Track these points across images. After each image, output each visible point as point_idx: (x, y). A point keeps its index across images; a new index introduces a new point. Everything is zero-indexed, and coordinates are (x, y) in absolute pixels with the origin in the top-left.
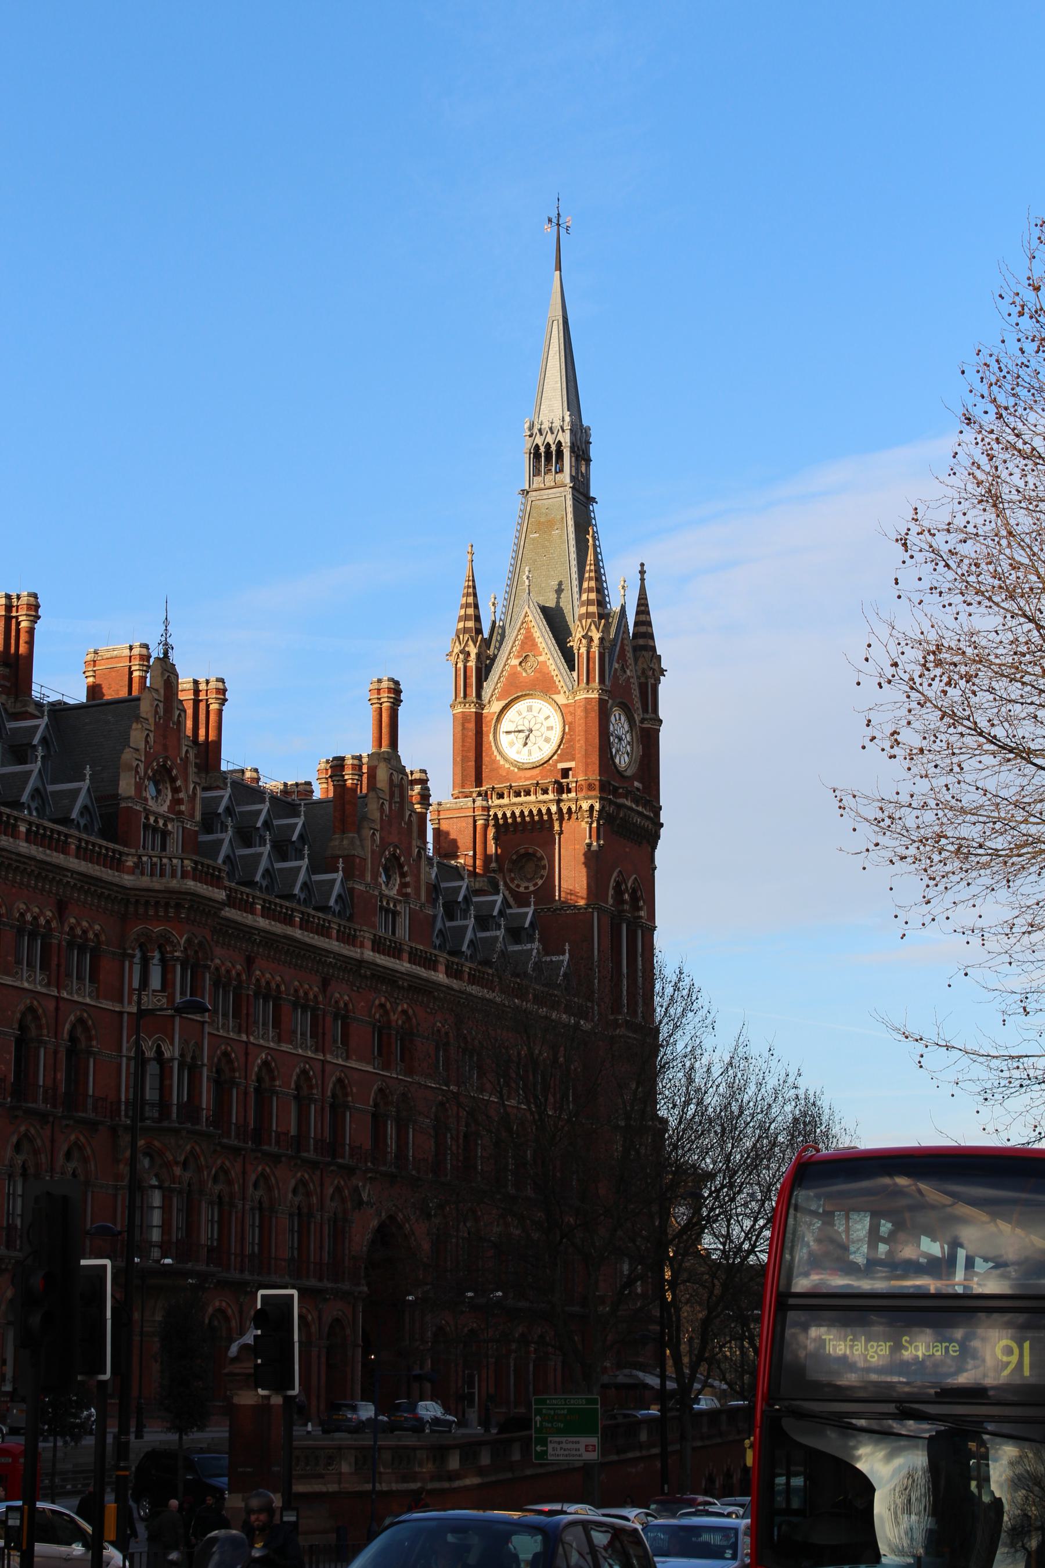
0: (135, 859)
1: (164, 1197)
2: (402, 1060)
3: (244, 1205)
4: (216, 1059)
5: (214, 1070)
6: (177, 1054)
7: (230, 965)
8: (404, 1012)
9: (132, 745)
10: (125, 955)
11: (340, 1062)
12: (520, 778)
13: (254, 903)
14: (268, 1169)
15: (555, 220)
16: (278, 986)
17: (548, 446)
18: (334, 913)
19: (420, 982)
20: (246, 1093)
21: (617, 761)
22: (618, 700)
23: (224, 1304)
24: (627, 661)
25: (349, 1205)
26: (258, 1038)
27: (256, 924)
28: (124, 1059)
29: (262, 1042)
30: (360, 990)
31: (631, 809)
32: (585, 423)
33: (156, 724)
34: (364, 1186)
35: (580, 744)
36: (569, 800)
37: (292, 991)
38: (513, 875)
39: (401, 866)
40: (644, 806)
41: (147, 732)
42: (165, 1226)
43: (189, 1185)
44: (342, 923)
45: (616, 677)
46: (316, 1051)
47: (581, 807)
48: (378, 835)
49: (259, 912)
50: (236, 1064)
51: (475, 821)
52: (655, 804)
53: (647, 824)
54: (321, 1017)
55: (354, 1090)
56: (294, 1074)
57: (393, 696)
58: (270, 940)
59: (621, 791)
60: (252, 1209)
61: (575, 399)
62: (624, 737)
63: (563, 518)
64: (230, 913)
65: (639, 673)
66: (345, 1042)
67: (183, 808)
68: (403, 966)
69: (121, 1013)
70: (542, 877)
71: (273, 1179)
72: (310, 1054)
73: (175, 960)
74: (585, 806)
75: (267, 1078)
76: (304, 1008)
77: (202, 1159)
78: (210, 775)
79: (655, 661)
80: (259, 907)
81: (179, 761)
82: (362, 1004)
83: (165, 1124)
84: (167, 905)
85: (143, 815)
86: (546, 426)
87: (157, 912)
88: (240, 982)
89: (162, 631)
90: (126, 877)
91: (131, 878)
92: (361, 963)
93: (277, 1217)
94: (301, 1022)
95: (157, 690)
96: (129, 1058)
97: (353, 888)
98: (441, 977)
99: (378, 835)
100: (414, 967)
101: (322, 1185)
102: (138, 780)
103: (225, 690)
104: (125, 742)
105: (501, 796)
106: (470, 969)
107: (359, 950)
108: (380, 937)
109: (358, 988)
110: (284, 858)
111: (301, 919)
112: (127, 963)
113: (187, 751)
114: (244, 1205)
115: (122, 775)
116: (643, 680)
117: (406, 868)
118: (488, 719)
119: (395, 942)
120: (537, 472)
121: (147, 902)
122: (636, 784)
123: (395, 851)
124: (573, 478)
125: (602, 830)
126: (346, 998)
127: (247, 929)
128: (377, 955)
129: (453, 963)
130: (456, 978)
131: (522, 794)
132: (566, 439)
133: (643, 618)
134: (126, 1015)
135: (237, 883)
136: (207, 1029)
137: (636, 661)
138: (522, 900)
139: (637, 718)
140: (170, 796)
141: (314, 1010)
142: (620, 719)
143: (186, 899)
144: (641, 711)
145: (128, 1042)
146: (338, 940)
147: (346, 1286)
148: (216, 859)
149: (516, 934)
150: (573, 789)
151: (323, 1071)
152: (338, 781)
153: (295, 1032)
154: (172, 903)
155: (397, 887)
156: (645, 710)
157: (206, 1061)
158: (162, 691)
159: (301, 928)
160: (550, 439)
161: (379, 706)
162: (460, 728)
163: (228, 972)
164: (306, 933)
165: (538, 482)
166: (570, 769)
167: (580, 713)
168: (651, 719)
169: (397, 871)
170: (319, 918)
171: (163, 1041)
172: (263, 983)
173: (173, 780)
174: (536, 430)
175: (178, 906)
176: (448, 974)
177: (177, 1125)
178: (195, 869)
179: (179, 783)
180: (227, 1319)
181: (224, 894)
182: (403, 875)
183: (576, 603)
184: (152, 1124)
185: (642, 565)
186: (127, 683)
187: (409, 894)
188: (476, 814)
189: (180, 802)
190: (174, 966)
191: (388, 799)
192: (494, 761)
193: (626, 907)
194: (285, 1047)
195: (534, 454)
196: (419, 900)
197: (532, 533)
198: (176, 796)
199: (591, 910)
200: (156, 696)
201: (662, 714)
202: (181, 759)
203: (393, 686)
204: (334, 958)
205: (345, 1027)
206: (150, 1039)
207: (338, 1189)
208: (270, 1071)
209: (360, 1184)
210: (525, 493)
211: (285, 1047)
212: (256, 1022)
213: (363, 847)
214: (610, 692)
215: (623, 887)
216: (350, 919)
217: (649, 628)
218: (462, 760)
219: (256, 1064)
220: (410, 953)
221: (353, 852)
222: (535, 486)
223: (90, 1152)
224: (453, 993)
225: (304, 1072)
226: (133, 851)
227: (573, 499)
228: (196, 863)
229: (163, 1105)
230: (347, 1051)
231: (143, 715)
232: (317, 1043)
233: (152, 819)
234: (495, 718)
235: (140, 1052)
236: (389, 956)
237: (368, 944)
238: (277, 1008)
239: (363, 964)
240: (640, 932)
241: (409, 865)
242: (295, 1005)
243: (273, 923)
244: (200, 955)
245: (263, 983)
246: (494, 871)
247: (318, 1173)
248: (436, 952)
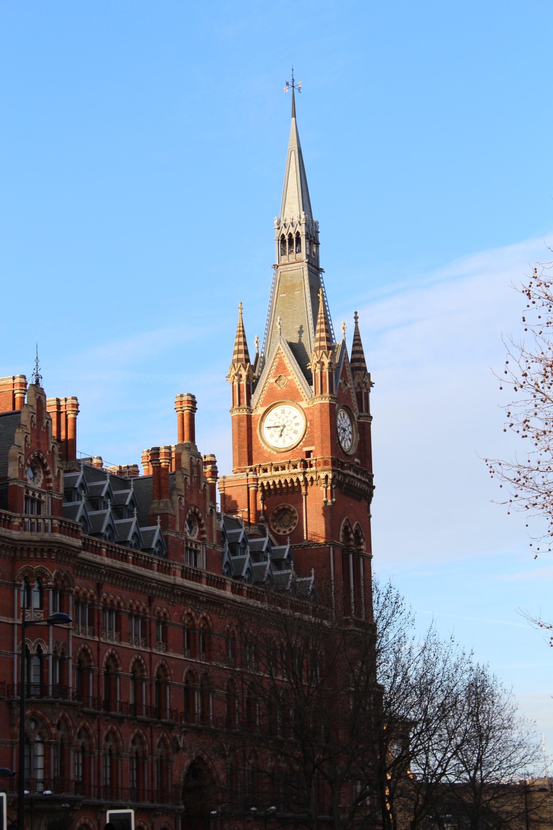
0: (20, 520)
1: (45, 749)
2: (204, 650)
3: (99, 752)
4: (78, 654)
5: (77, 661)
6: (51, 651)
7: (86, 590)
8: (204, 618)
9: (16, 443)
10: (15, 585)
11: (162, 653)
12: (278, 458)
13: (101, 548)
14: (115, 728)
15: (291, 84)
16: (119, 603)
17: (290, 235)
18: (155, 552)
19: (214, 597)
20: (99, 676)
21: (343, 445)
22: (343, 404)
23: (87, 820)
24: (347, 378)
25: (170, 750)
26: (106, 639)
27: (103, 562)
28: (16, 656)
29: (109, 641)
30: (174, 604)
31: (353, 477)
32: (315, 219)
33: (32, 429)
34: (180, 737)
35: (317, 434)
36: (311, 472)
37: (128, 606)
38: (275, 524)
39: (199, 520)
40: (362, 475)
41: (26, 434)
42: (46, 768)
43: (62, 740)
44: (162, 559)
45: (340, 389)
46: (146, 646)
47: (319, 477)
48: (183, 499)
49: (104, 553)
50: (92, 657)
51: (248, 488)
52: (369, 473)
53: (364, 487)
54: (148, 623)
55: (172, 672)
56: (131, 662)
57: (191, 405)
58: (112, 572)
59: (346, 465)
60: (105, 755)
61: (307, 203)
62: (347, 428)
63: (301, 283)
64: (84, 555)
65: (356, 385)
66: (165, 639)
67: (51, 485)
68: (202, 587)
69: (13, 624)
70: (294, 524)
71: (118, 734)
72: (141, 648)
73: (49, 588)
74: (322, 475)
75: (113, 666)
76: (137, 618)
77: (70, 722)
78: (70, 462)
79: (366, 377)
80: (104, 550)
81: (48, 454)
82: (176, 614)
83: (44, 699)
84: (42, 550)
85: (25, 490)
86: (288, 222)
87: (35, 556)
88: (93, 601)
89: (35, 367)
90: (14, 532)
91: (18, 533)
92: (174, 586)
93: (121, 760)
94: (135, 627)
95: (32, 406)
97: (168, 536)
98: (228, 594)
99: (183, 499)
100: (210, 587)
101: (152, 737)
102: (20, 467)
103: (77, 405)
104: (11, 441)
105: (265, 471)
106: (248, 587)
107: (172, 577)
108: (187, 568)
109: (173, 603)
110: (121, 517)
111: (133, 557)
112: (16, 591)
113: (53, 447)
114: (99, 752)
115: (10, 464)
116: (359, 390)
117: (203, 521)
118: (255, 419)
119: (197, 571)
120: (283, 253)
121: (29, 549)
122: (356, 460)
123: (195, 509)
124: (308, 256)
125: (334, 491)
126: (165, 610)
127: (96, 565)
128: (185, 580)
129: (236, 584)
130: (238, 594)
131: (280, 469)
132: (302, 230)
133: (357, 348)
134: (16, 626)
135: (89, 535)
136: (72, 633)
137: (354, 377)
138: (281, 540)
139: (356, 416)
140: (42, 477)
141: (143, 618)
142: (344, 417)
143: (55, 546)
144: (357, 411)
145: (18, 644)
146: (158, 571)
147: (169, 806)
148: (74, 519)
149: (278, 563)
150: (314, 465)
151: (151, 660)
152: (155, 464)
153: (130, 634)
154: (46, 549)
155: (197, 534)
156: (361, 410)
157: (71, 655)
158: (35, 407)
159: (133, 564)
160: (292, 230)
161: (181, 412)
162: (236, 426)
163: (85, 594)
164: (137, 567)
165: (284, 259)
166: (311, 451)
167: (317, 413)
168: (365, 416)
169: (197, 523)
170: (145, 556)
171: (42, 642)
172: (108, 601)
173: (44, 466)
174: (282, 225)
175: (50, 551)
176: (233, 592)
177: (52, 699)
178: (60, 526)
179: (48, 468)
181: (81, 542)
182: (201, 526)
183: (312, 340)
184: (36, 699)
185: (356, 313)
186: (11, 402)
187: (205, 538)
188: (249, 483)
189: (49, 481)
190: (48, 592)
191: (189, 474)
192: (260, 447)
193: (352, 543)
194: (124, 644)
195: (281, 241)
196: (212, 542)
197: (281, 294)
198: (47, 477)
199: (328, 546)
200: (31, 410)
201: (372, 413)
202: (49, 452)
203: (190, 399)
204: (156, 583)
205: (165, 629)
206: (33, 641)
207: (163, 740)
208: (115, 660)
209: (178, 736)
210: (276, 267)
211: (124, 644)
212: (104, 628)
213: (173, 508)
214: (337, 399)
215: (350, 530)
216: (166, 556)
217: (362, 355)
218: (239, 447)
219: (105, 656)
220: (207, 578)
221: (167, 512)
222: (282, 262)
224: (236, 604)
225: (138, 661)
226: (18, 515)
227: (309, 270)
228: (61, 521)
229: (43, 686)
230: (167, 646)
231: (23, 423)
232: (146, 641)
233: (31, 493)
234: (260, 418)
236: (193, 580)
237: (179, 573)
238: (118, 618)
239: (176, 587)
240: (361, 560)
241: (205, 519)
242: (131, 615)
243: (114, 560)
244: (66, 584)
245: (108, 601)
246: (262, 521)
247: (149, 729)
248: (225, 577)
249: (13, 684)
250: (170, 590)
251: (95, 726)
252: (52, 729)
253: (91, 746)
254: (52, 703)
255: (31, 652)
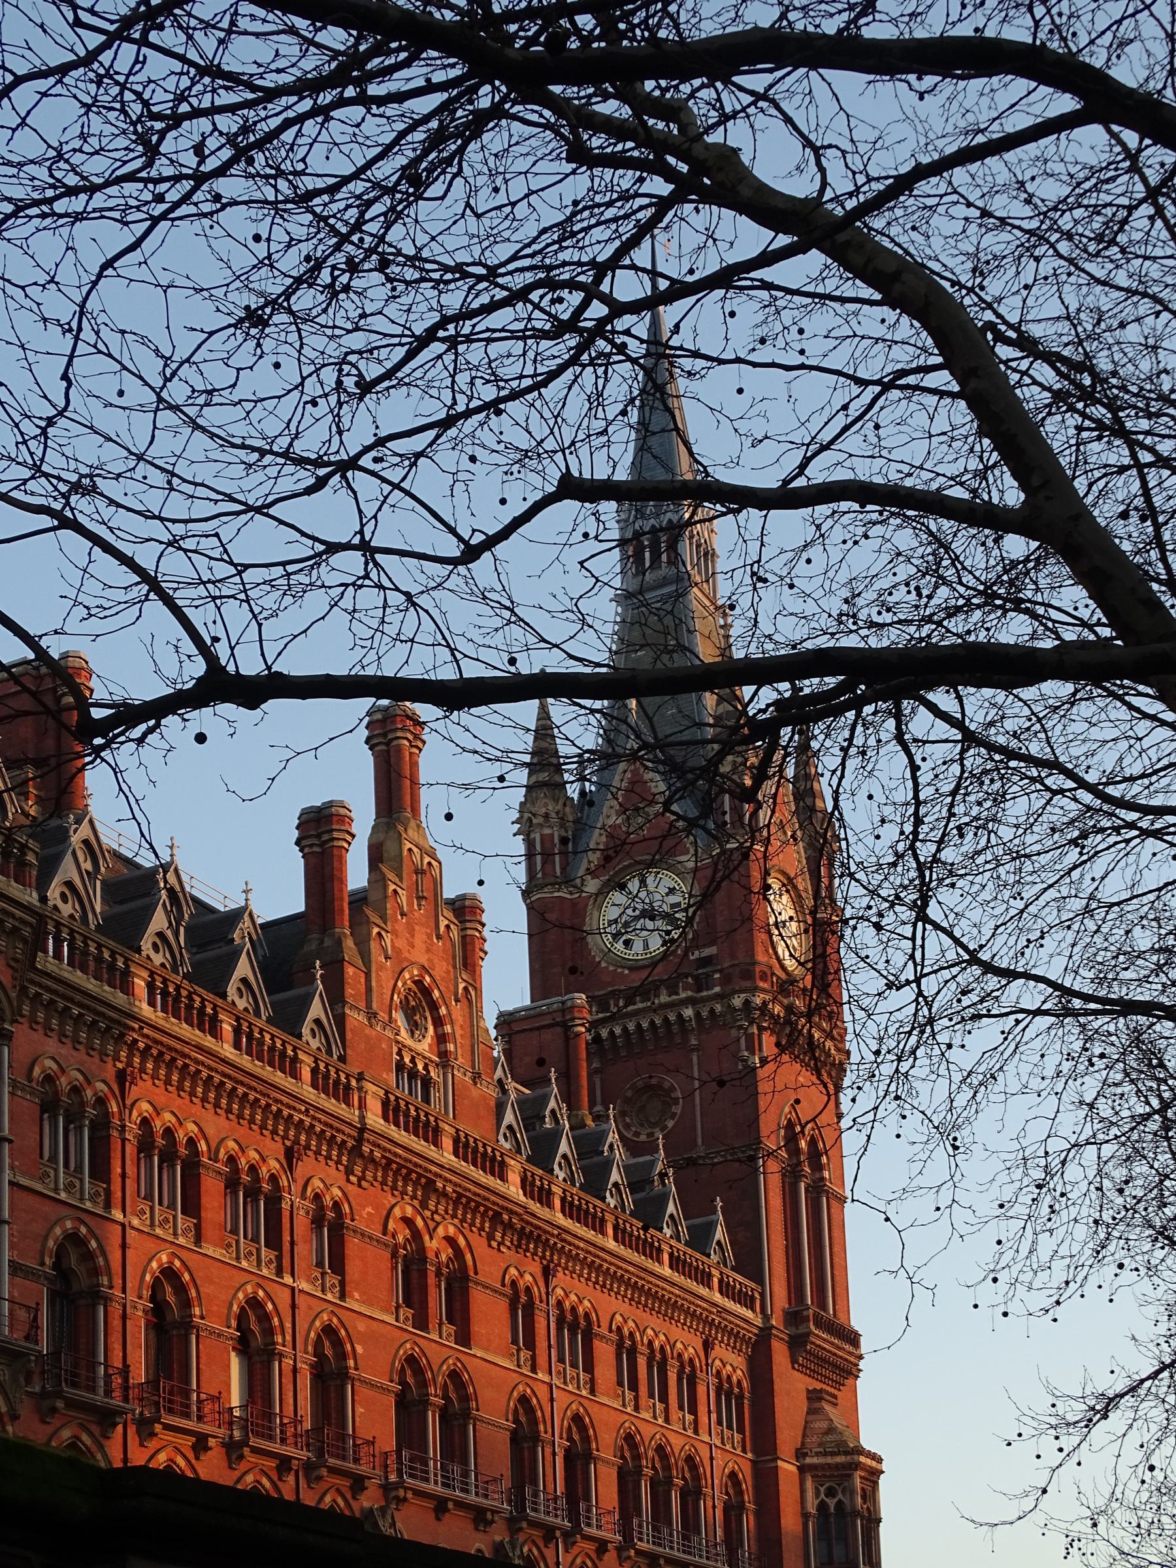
39: (434, 1007)
55: (359, 1349)
66: (338, 1265)
70: (673, 1116)
82: (369, 1209)
109: (359, 1180)
126: (337, 1192)
161: (383, 747)
182: (438, 1022)
232: (279, 1259)
250: (351, 1143)
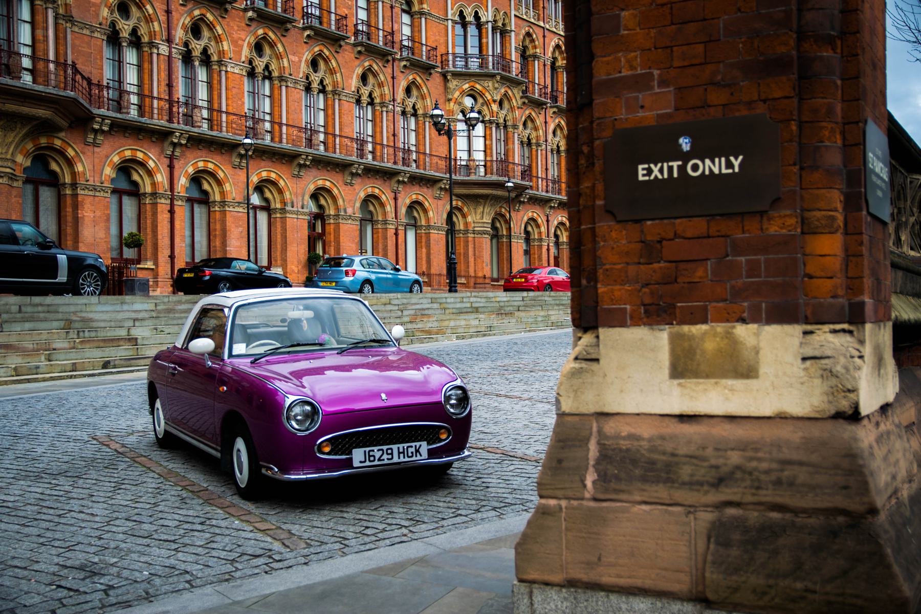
6: (490, 19)
23: (535, 215)
50: (537, 43)
96: (455, 22)
145: (452, 9)
180: (538, 226)
206: (469, 6)
223: (426, 91)
235: (461, 15)
249: (448, 54)
251: (542, 117)
252: (493, 105)
253: (538, 137)
254: (492, 76)
255: (467, 20)
